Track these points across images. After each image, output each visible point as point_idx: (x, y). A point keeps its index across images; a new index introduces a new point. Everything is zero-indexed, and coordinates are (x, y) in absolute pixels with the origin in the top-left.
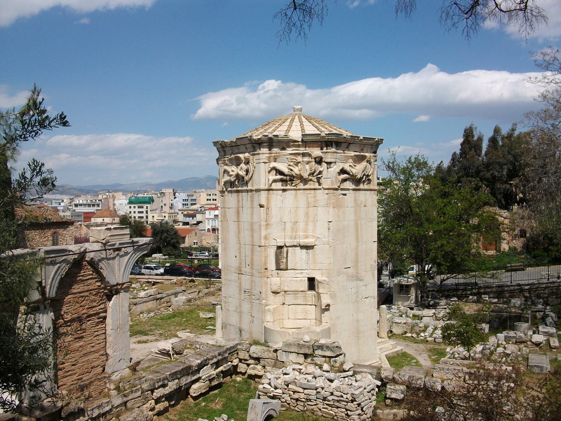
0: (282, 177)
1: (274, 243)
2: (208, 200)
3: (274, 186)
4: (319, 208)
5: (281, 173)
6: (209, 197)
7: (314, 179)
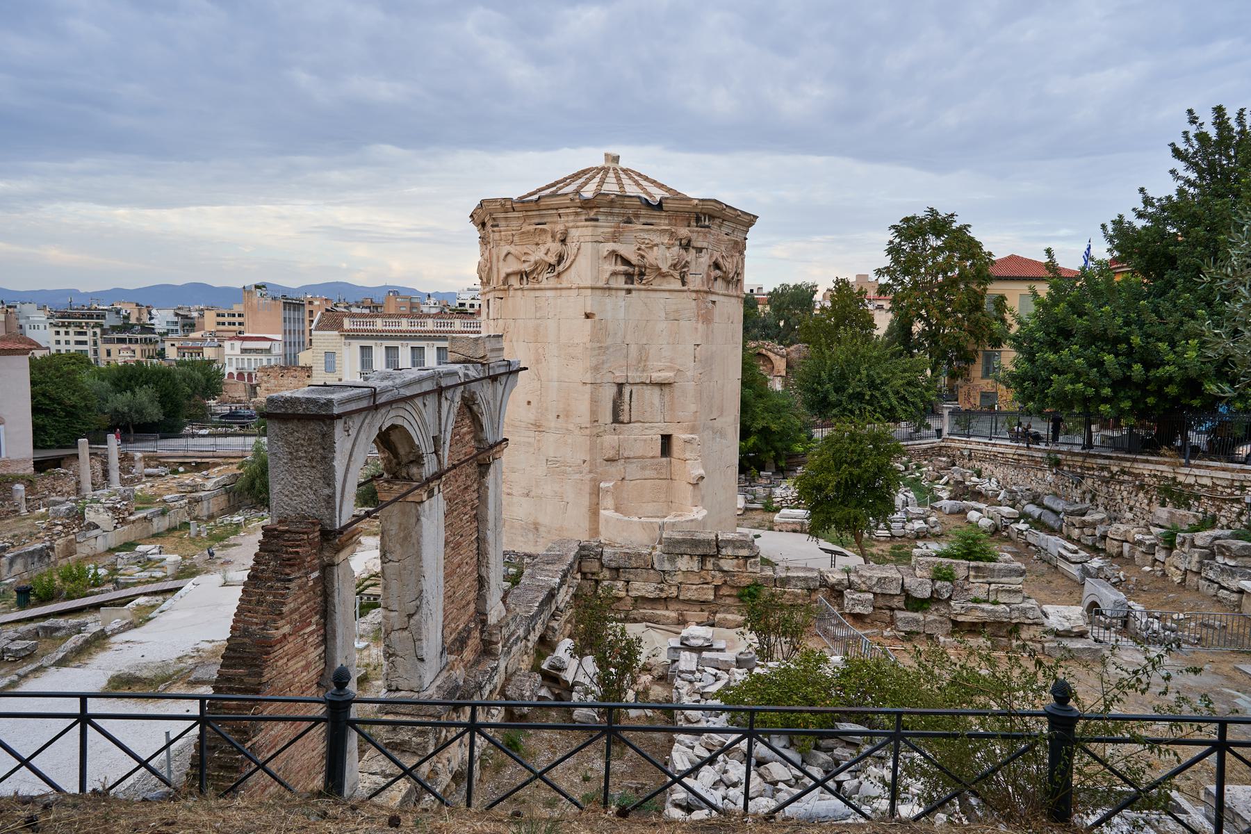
0: (626, 268)
1: (609, 377)
2: (218, 323)
3: (613, 284)
4: (682, 322)
5: (626, 262)
6: (221, 319)
7: (676, 274)
